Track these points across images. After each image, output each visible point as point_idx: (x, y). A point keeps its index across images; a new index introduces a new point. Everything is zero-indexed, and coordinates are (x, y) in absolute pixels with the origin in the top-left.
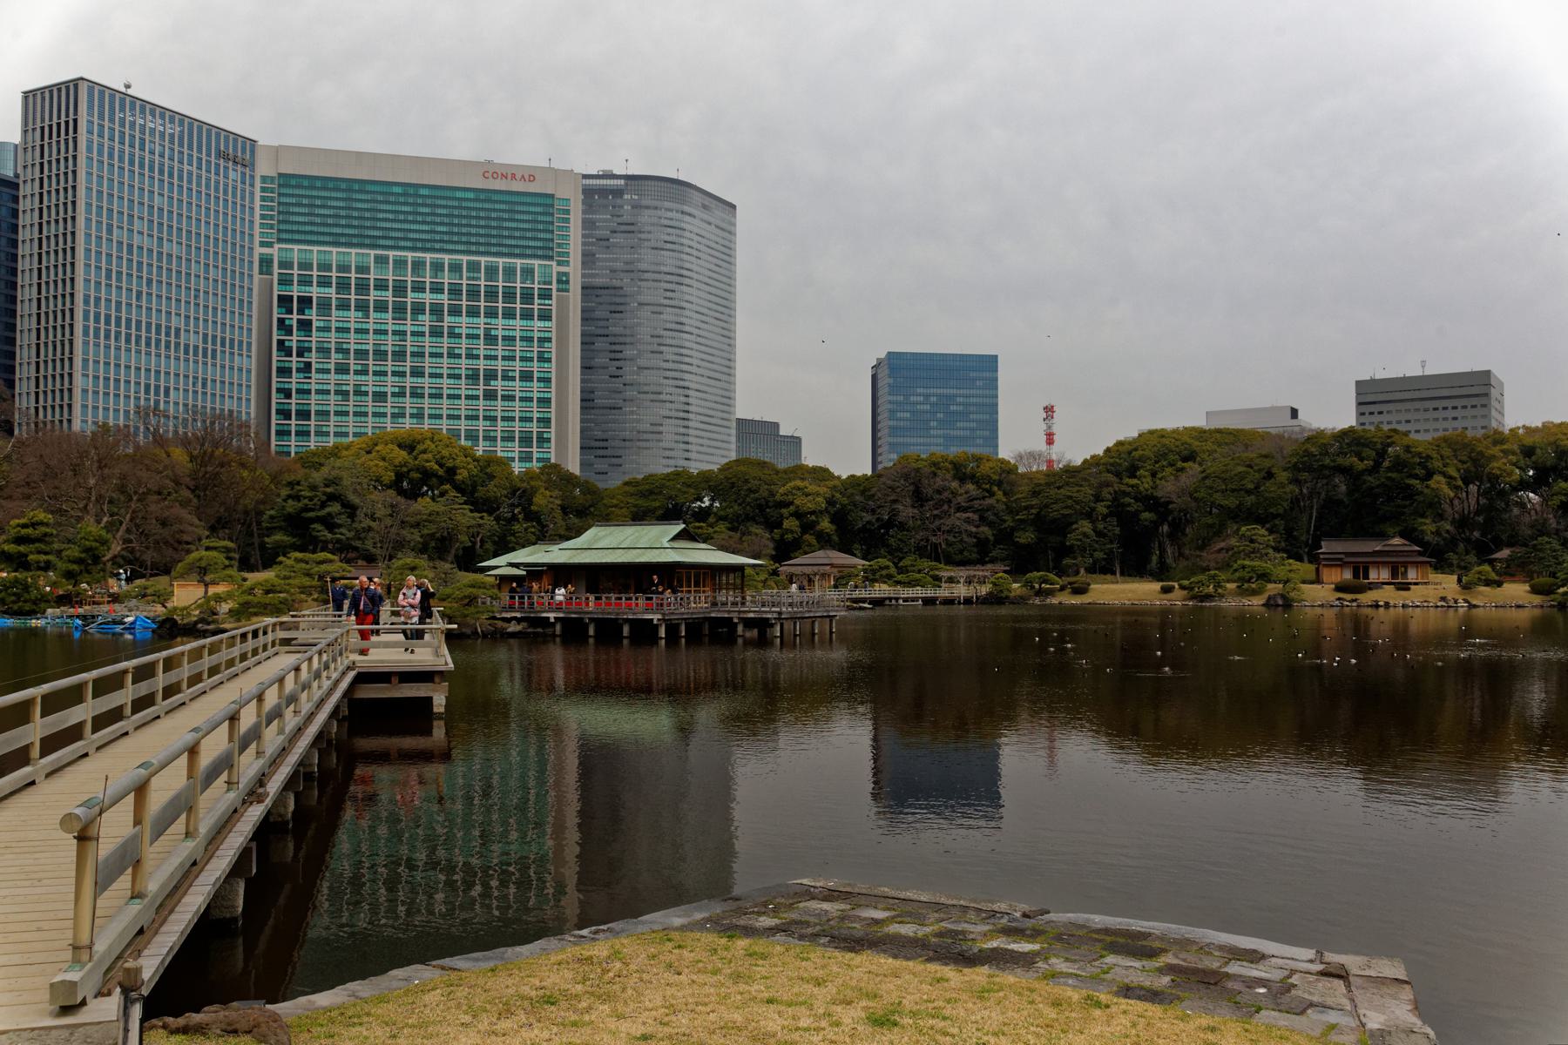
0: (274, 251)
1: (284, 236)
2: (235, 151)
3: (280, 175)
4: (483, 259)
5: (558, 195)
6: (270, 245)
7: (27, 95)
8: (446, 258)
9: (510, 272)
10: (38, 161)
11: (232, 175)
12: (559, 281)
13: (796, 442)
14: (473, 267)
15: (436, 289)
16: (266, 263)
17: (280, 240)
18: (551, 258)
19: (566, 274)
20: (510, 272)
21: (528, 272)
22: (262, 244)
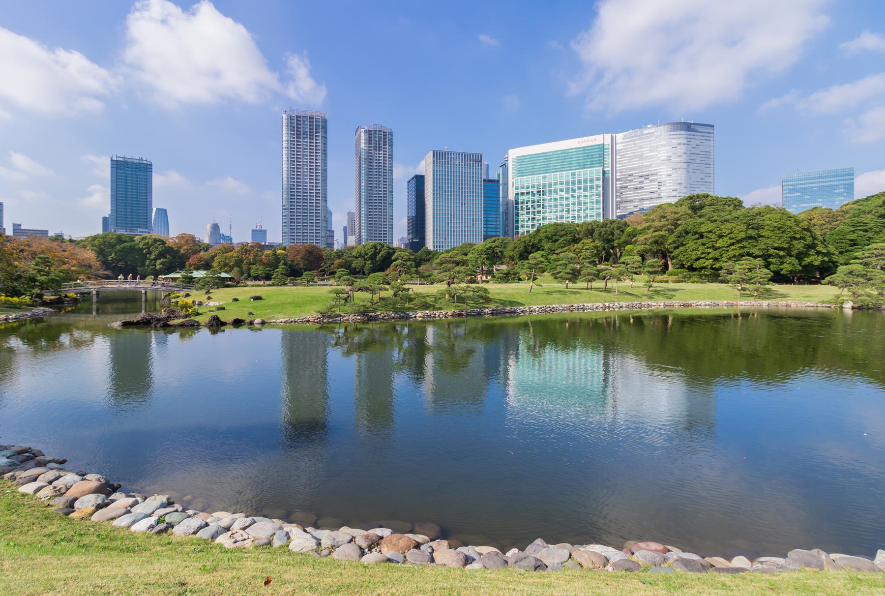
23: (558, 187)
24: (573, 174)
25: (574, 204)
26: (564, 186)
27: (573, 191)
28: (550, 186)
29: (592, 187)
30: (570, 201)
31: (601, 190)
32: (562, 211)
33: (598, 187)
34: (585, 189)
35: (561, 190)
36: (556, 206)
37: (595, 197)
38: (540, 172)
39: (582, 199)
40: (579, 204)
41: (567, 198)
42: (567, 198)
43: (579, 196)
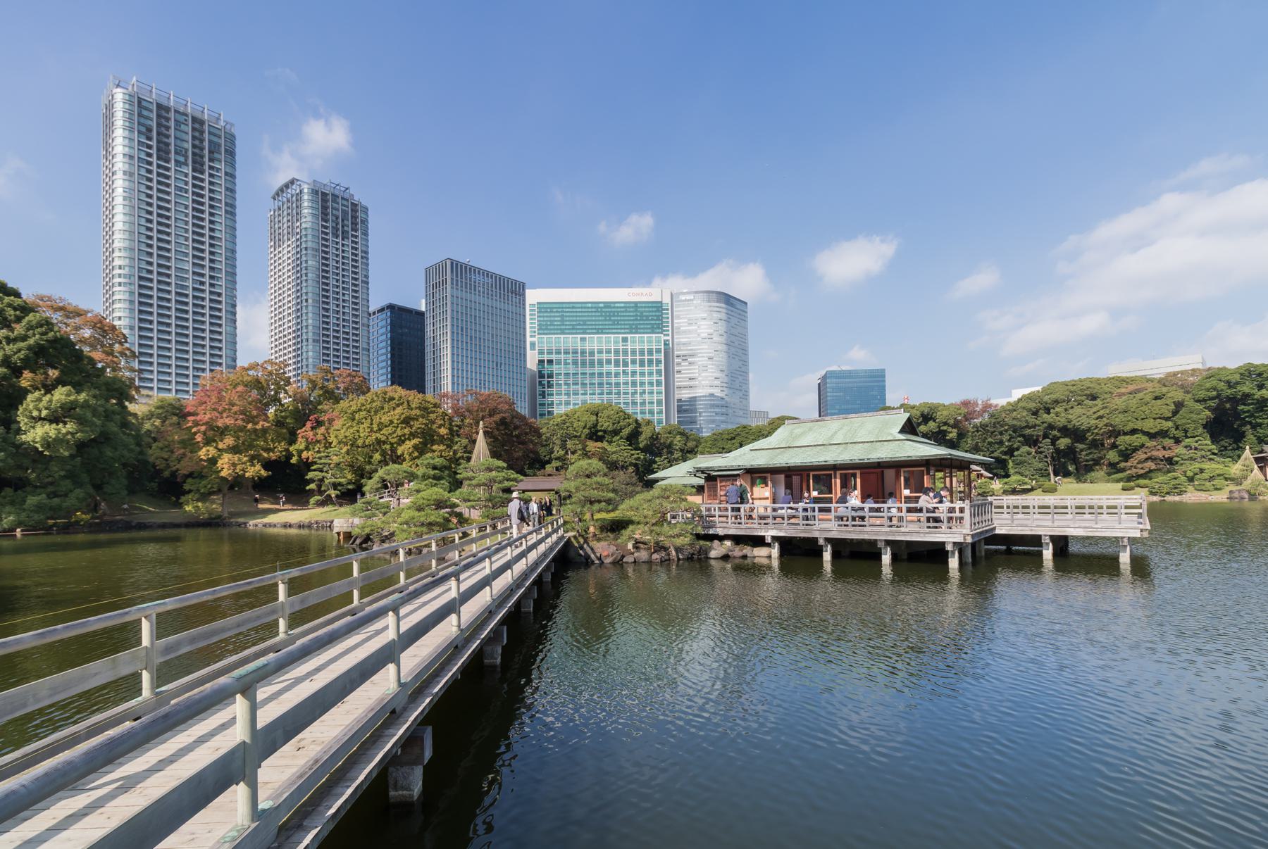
7: (428, 270)
23: (604, 357)
24: (625, 340)
25: (626, 384)
26: (613, 357)
27: (625, 364)
28: (592, 354)
29: (650, 362)
30: (622, 379)
31: (662, 367)
32: (610, 393)
33: (659, 362)
34: (642, 364)
35: (609, 362)
36: (601, 385)
37: (655, 377)
38: (573, 330)
39: (638, 378)
40: (634, 384)
41: (617, 375)
42: (617, 375)
43: (634, 373)
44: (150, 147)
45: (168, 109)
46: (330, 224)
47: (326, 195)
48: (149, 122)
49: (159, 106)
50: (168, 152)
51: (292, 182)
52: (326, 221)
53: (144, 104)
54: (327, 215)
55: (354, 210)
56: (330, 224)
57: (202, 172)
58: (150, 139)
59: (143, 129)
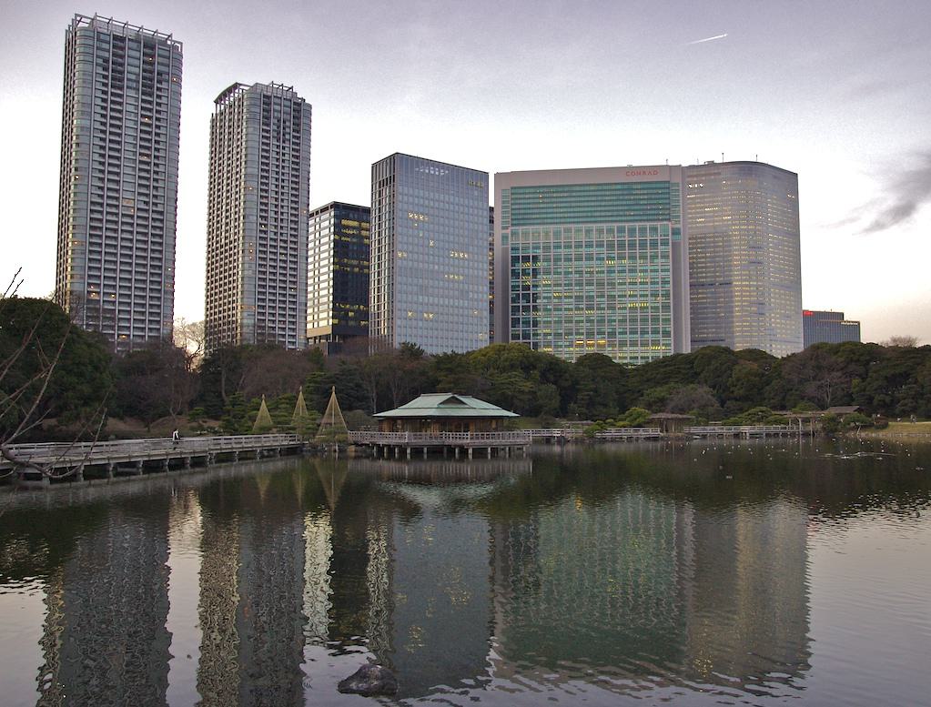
0: (509, 231)
1: (515, 222)
2: (476, 179)
3: (512, 188)
4: (627, 225)
5: (672, 181)
6: (507, 228)
7: (375, 166)
8: (605, 226)
9: (643, 230)
10: (378, 199)
11: (476, 193)
12: (673, 234)
13: (856, 327)
14: (621, 230)
15: (600, 245)
16: (505, 237)
17: (512, 225)
18: (669, 220)
19: (679, 229)
20: (643, 230)
21: (654, 229)
22: (503, 228)
44: (105, 77)
45: (122, 39)
46: (273, 127)
47: (269, 97)
48: (106, 55)
49: (116, 37)
50: (121, 80)
51: (236, 86)
52: (268, 125)
53: (102, 37)
54: (268, 118)
55: (299, 111)
56: (273, 127)
57: (151, 95)
58: (105, 69)
59: (100, 61)
